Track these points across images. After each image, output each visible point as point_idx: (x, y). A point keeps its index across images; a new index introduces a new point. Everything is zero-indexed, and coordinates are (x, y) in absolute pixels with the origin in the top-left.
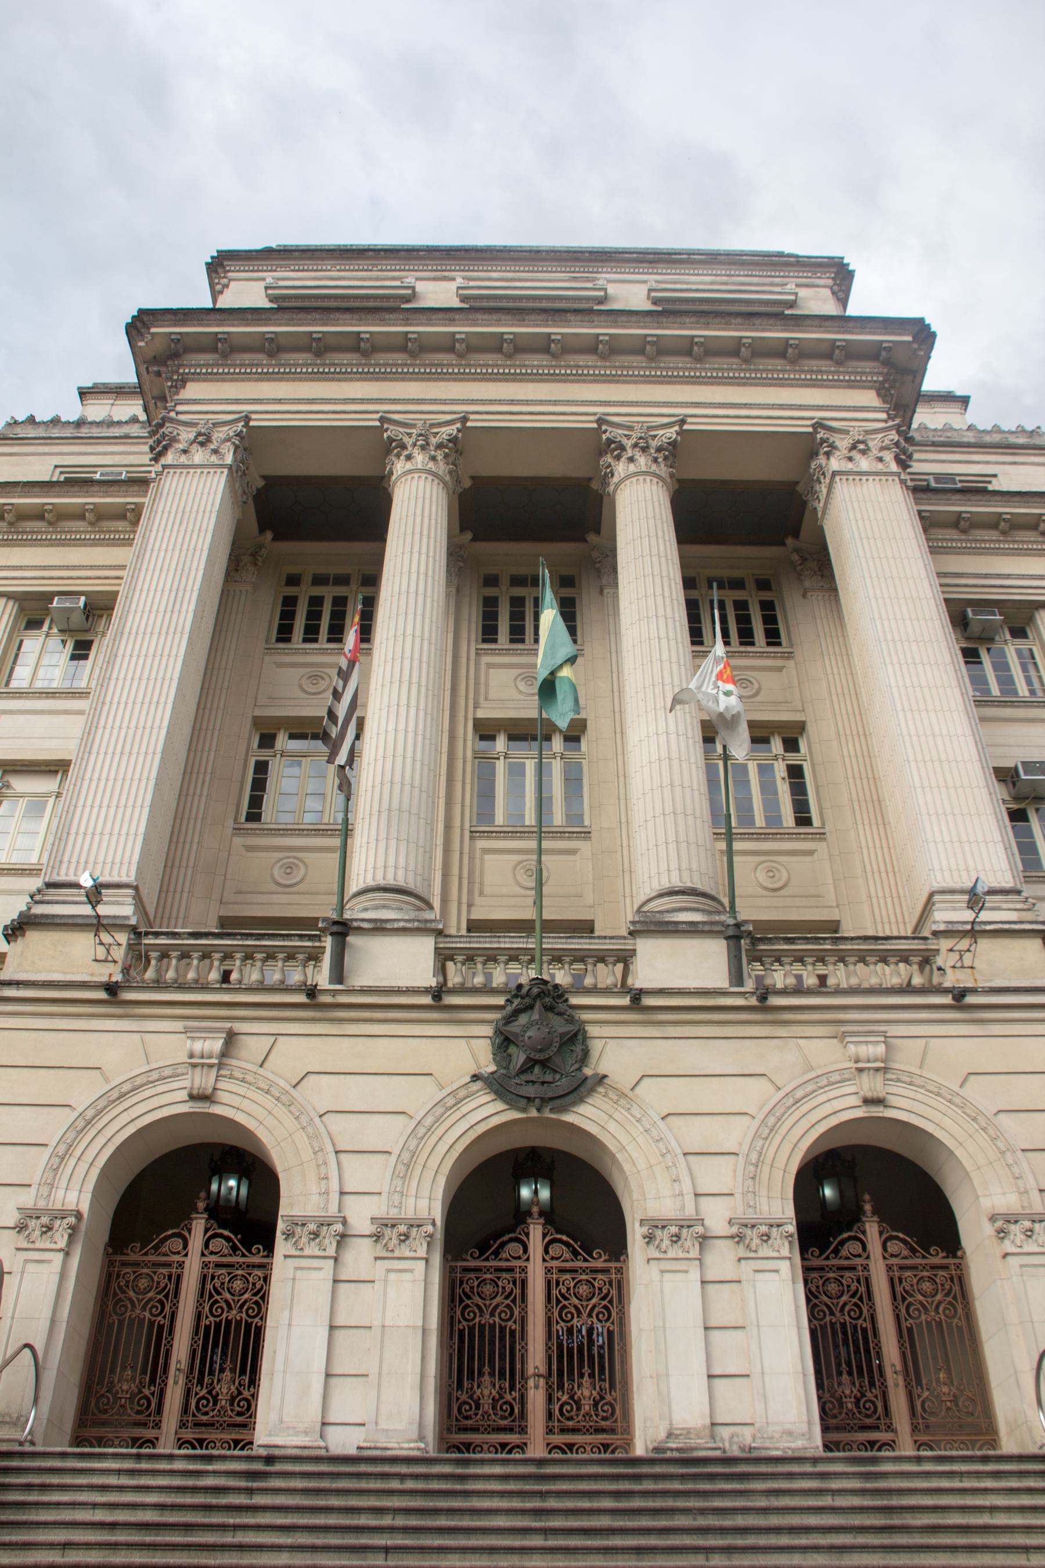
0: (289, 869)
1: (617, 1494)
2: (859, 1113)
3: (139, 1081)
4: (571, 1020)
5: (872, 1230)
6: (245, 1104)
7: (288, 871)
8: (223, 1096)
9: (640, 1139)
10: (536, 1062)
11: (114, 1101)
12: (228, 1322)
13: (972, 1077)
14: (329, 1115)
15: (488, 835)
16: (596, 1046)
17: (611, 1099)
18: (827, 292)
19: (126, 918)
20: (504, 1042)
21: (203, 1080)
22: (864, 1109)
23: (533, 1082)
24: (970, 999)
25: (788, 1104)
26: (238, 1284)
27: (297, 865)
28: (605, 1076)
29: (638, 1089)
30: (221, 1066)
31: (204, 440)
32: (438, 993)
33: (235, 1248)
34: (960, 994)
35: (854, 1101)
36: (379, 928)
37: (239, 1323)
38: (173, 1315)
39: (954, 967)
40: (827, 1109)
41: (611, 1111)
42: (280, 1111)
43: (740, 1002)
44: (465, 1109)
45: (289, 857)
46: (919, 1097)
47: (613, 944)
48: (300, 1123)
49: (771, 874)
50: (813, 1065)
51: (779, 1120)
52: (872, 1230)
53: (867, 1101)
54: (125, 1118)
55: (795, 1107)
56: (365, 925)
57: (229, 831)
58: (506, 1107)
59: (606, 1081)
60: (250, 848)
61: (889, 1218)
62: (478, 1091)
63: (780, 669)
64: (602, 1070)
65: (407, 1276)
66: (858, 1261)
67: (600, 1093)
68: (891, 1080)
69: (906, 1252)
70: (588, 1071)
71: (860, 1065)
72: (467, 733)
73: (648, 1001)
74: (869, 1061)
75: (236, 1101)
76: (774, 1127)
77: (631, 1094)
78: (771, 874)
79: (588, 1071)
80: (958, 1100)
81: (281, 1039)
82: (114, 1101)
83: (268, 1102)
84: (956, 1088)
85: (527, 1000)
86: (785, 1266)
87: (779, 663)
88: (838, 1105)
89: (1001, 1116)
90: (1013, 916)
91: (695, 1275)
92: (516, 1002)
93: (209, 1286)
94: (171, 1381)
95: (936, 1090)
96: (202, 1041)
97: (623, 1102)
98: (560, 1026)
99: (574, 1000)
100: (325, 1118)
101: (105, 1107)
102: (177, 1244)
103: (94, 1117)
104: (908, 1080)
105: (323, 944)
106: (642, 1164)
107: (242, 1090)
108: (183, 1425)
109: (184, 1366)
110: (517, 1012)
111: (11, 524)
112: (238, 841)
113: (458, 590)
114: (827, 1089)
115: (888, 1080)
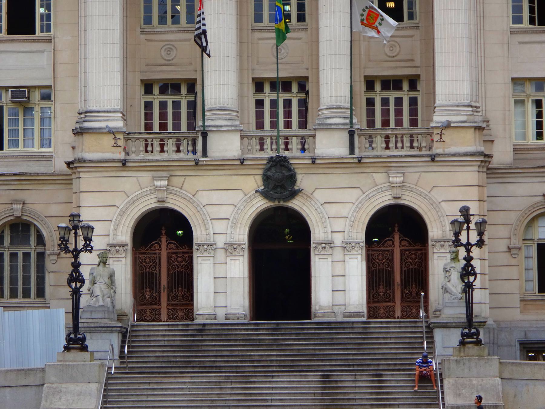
0: (169, 51)
1: (297, 334)
3: (139, 196)
4: (290, 170)
5: (397, 237)
6: (177, 203)
7: (169, 53)
8: (169, 200)
9: (314, 213)
10: (278, 186)
11: (131, 204)
12: (178, 272)
13: (435, 188)
14: (207, 206)
15: (260, 31)
16: (299, 177)
17: (305, 198)
19: (121, 128)
20: (266, 179)
21: (162, 195)
22: (394, 200)
23: (277, 193)
24: (437, 159)
25: (366, 199)
26: (180, 259)
27: (171, 49)
28: (302, 190)
29: (314, 194)
30: (167, 189)
32: (242, 162)
33: (177, 247)
36: (219, 130)
37: (182, 272)
38: (160, 270)
39: (437, 141)
41: (304, 202)
42: (190, 205)
43: (351, 161)
44: (254, 203)
45: (168, 44)
46: (414, 196)
47: (307, 133)
48: (197, 210)
49: (391, 49)
50: (377, 184)
51: (363, 205)
52: (397, 237)
53: (395, 198)
54: (136, 210)
55: (368, 200)
56: (214, 129)
57: (139, 32)
58: (268, 201)
59: (302, 191)
61: (404, 233)
62: (258, 196)
64: (301, 187)
65: (238, 261)
66: (390, 248)
67: (300, 196)
68: (404, 190)
69: (408, 245)
70: (296, 188)
71: (393, 185)
73: (317, 161)
74: (396, 184)
75: (174, 202)
76: (360, 208)
77: (311, 196)
78: (391, 49)
79: (296, 188)
80: (427, 197)
81: (187, 177)
82: (131, 204)
83: (186, 203)
84: (427, 193)
85: (274, 163)
86: (359, 257)
88: (384, 199)
89: (442, 203)
90: (464, 118)
91: (330, 260)
92: (271, 163)
93: (170, 260)
94: (162, 291)
95: (420, 194)
96: (160, 181)
97: (308, 199)
98: (287, 173)
99: (291, 162)
100: (206, 207)
101: (129, 206)
102: (157, 246)
103: (126, 210)
104: (410, 190)
105: (198, 136)
106: (314, 222)
107: (176, 198)
108: (168, 304)
109: (166, 286)
110: (271, 167)
112: (143, 36)
114: (381, 193)
115: (403, 190)
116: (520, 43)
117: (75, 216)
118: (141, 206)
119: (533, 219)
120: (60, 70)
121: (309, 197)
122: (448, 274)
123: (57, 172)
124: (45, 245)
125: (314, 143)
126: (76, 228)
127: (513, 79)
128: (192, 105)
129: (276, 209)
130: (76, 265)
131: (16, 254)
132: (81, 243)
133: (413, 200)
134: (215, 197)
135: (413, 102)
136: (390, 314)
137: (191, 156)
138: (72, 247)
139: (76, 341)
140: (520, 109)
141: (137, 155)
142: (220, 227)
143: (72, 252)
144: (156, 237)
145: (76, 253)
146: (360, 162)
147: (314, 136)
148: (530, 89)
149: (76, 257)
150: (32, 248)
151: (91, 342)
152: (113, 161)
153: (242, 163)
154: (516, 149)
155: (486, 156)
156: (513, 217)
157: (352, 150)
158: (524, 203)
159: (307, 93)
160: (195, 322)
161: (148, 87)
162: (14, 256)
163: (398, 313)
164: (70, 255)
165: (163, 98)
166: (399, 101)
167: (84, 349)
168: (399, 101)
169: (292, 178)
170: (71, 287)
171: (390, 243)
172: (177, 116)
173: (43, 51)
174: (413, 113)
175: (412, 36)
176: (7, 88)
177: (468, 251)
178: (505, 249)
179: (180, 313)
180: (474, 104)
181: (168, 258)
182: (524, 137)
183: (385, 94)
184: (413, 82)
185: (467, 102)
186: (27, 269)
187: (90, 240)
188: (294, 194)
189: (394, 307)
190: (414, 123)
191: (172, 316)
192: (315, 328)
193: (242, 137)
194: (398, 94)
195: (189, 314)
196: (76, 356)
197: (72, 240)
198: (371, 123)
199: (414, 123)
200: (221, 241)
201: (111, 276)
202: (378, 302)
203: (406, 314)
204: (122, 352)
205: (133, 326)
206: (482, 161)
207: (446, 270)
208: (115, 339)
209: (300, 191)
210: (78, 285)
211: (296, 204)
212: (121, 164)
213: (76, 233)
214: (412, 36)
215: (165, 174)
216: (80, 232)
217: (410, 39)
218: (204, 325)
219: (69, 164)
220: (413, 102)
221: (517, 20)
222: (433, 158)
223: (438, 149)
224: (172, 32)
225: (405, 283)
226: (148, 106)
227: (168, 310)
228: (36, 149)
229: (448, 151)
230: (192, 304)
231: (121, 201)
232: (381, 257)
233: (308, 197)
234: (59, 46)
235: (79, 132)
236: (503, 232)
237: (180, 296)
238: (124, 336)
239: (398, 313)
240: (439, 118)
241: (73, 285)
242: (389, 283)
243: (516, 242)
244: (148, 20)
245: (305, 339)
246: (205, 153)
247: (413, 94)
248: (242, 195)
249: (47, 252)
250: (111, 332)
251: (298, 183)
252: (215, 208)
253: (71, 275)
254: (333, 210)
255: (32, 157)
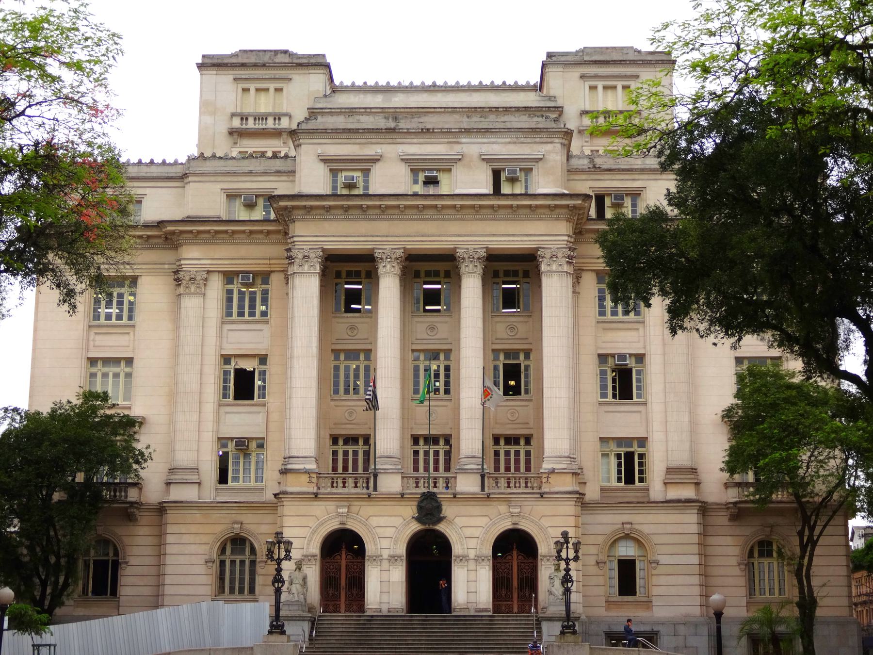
0: (351, 413)
2: (511, 527)
4: (437, 502)
5: (515, 553)
6: (354, 525)
16: (444, 508)
18: (559, 146)
20: (420, 508)
21: (344, 519)
24: (545, 496)
26: (355, 567)
31: (306, 257)
32: (402, 495)
34: (542, 495)
35: (510, 523)
36: (386, 472)
38: (340, 575)
40: (503, 526)
42: (364, 527)
52: (515, 553)
53: (514, 524)
54: (324, 530)
60: (337, 406)
61: (520, 550)
63: (526, 322)
64: (445, 515)
70: (442, 515)
72: (410, 356)
73: (457, 496)
75: (352, 524)
79: (442, 515)
86: (487, 567)
87: (526, 319)
88: (506, 524)
98: (435, 505)
106: (454, 540)
111: (213, 236)
112: (332, 403)
113: (404, 288)
116: (606, 412)
117: (279, 534)
118: (328, 527)
119: (615, 541)
120: (272, 426)
121: (451, 522)
122: (552, 581)
123: (267, 501)
124: (256, 555)
125: (456, 483)
126: (279, 542)
127: (601, 438)
128: (367, 454)
129: (426, 531)
130: (279, 570)
131: (235, 561)
132: (283, 554)
133: (527, 526)
134: (382, 521)
135: (528, 453)
136: (509, 610)
137: (365, 491)
138: (276, 557)
139: (277, 627)
140: (605, 460)
141: (326, 489)
142: (385, 543)
143: (276, 561)
144: (339, 550)
145: (279, 561)
146: (488, 497)
147: (455, 478)
148: (613, 446)
149: (279, 564)
150: (247, 557)
151: (289, 628)
152: (308, 493)
153: (402, 497)
154: (603, 490)
155: (580, 494)
156: (600, 539)
157: (483, 489)
158: (608, 529)
159: (451, 446)
160: (366, 614)
161: (335, 440)
162: (233, 562)
163: (516, 609)
164: (274, 562)
165: (346, 448)
166: (517, 453)
167: (283, 633)
168: (517, 453)
169: (439, 508)
170: (274, 586)
171: (510, 557)
172: (355, 461)
173: (259, 413)
174: (528, 461)
175: (527, 406)
176: (232, 439)
177: (567, 564)
178: (594, 563)
179: (355, 607)
180: (572, 456)
181: (346, 566)
182: (609, 480)
183: (508, 448)
184: (528, 440)
185: (567, 454)
186: (242, 572)
187: (290, 552)
188: (440, 520)
189: (512, 605)
190: (528, 469)
191: (349, 609)
192: (454, 620)
193: (403, 478)
194: (517, 448)
195: (361, 608)
196: (277, 639)
197: (276, 551)
198: (497, 469)
199: (528, 469)
200: (385, 554)
201: (305, 579)
202: (501, 601)
203: (521, 610)
204: (311, 635)
205: (320, 616)
206: (577, 498)
207: (551, 578)
208: (306, 626)
209: (444, 518)
210: (280, 585)
211: (441, 527)
212: (314, 496)
213: (279, 547)
214: (527, 406)
215: (346, 503)
216: (282, 546)
217: (526, 408)
218: (372, 616)
219: (275, 495)
220: (528, 453)
221: (604, 395)
222: (542, 495)
223: (545, 488)
224: (354, 400)
225: (521, 588)
226: (335, 453)
227: (346, 604)
228: (252, 484)
229: (553, 490)
230: (364, 601)
231: (313, 523)
232: (503, 567)
233: (450, 522)
234: (271, 410)
235: (284, 472)
236: (593, 550)
237: (355, 595)
238: (313, 624)
239: (516, 609)
240: (546, 466)
241: (276, 585)
242: (509, 588)
243: (602, 558)
244: (336, 391)
245: (447, 628)
246: (375, 489)
247: (528, 448)
248: (402, 520)
249: (258, 560)
250: (304, 620)
251: (443, 512)
252: (382, 530)
253: (275, 578)
254: (468, 532)
255: (249, 489)
